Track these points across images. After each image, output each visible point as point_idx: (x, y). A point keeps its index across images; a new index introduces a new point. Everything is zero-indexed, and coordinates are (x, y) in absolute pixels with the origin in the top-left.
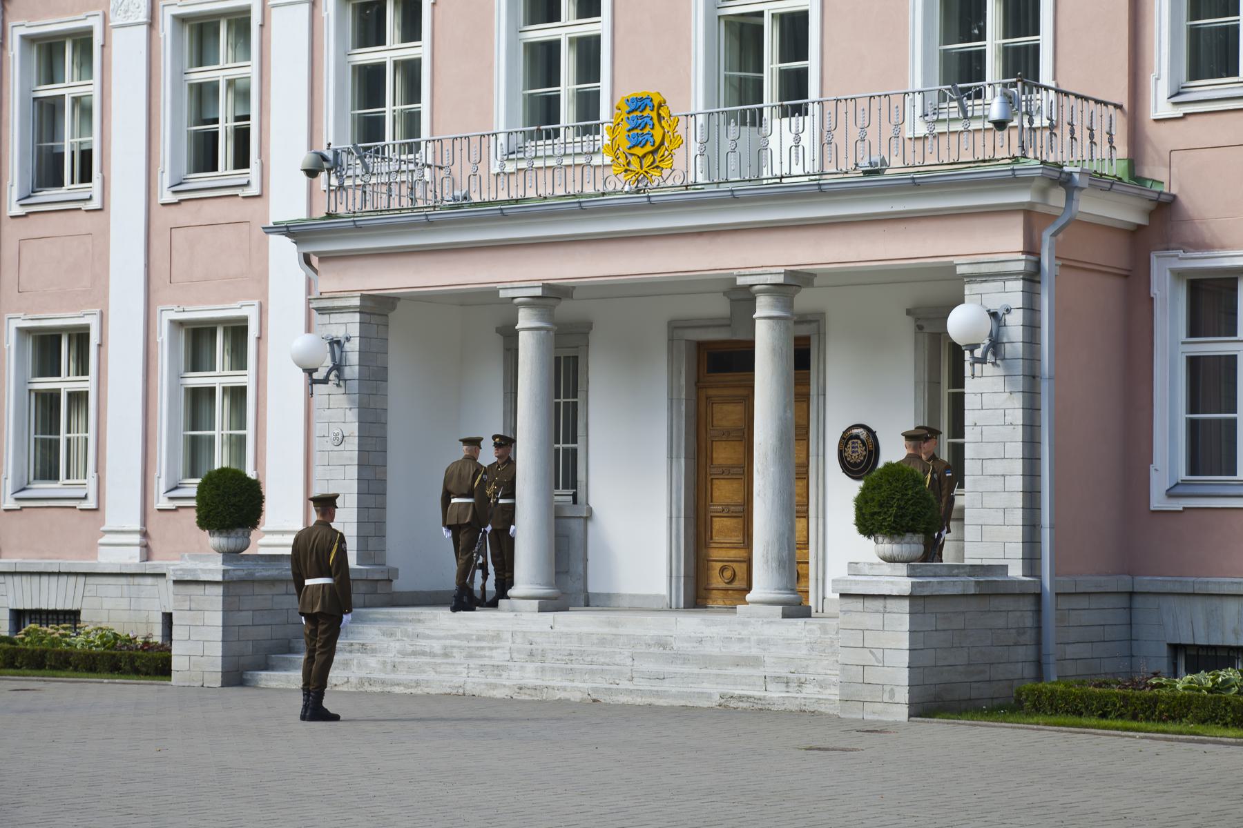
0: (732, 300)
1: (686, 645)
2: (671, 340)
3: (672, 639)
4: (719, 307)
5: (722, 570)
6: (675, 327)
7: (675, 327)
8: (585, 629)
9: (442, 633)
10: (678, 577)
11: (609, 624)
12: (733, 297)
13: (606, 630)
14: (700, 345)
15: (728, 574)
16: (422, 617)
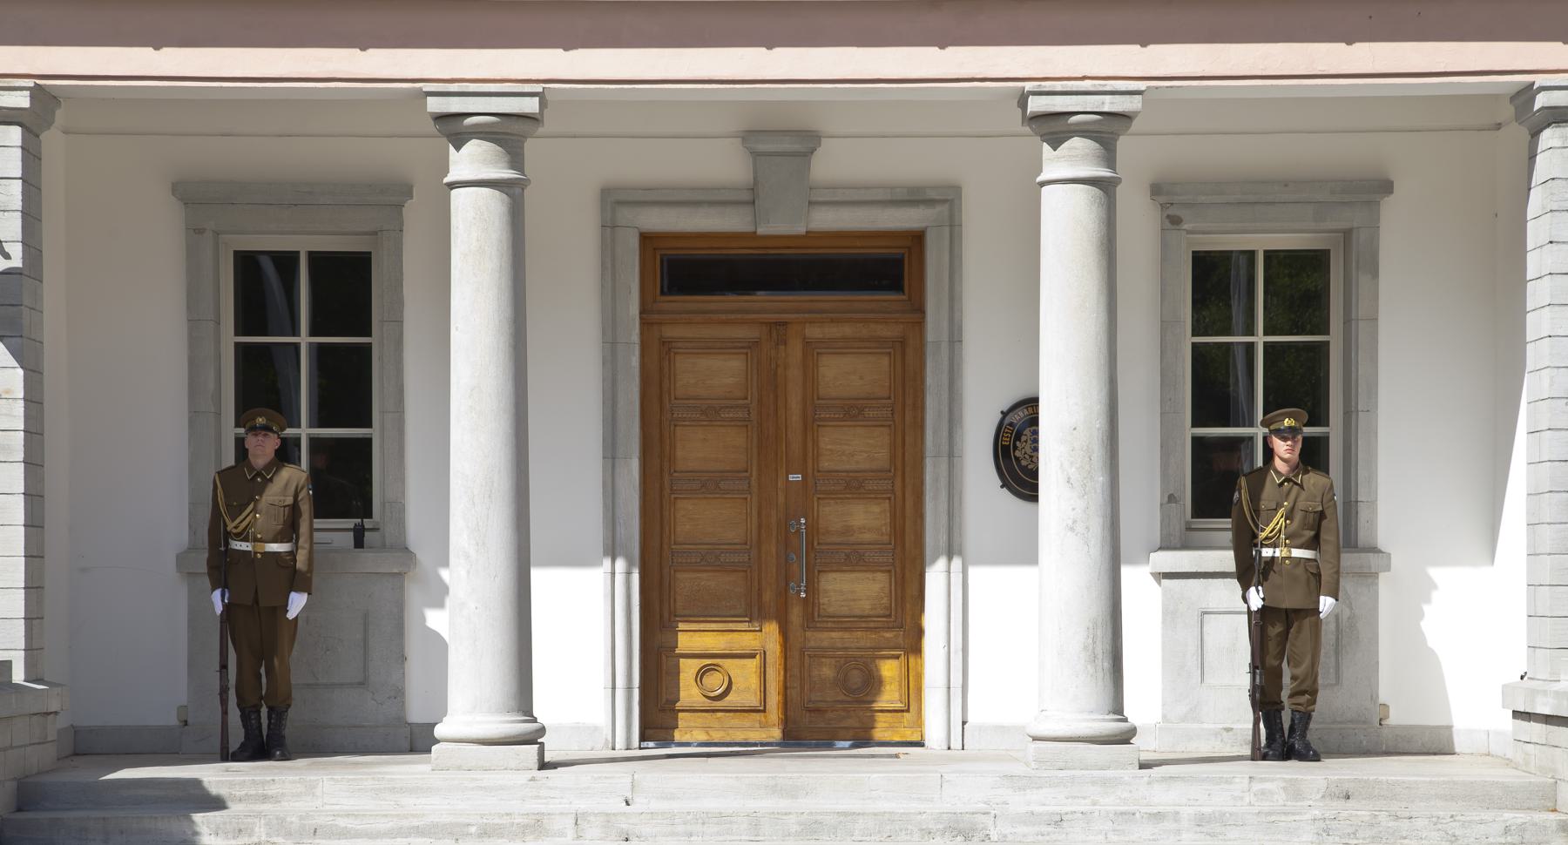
0: (756, 155)
1: (1022, 829)
2: (609, 227)
3: (989, 821)
4: (724, 165)
5: (701, 674)
6: (614, 200)
7: (614, 200)
8: (711, 804)
9: (383, 825)
10: (629, 688)
11: (775, 790)
12: (762, 147)
13: (766, 804)
14: (648, 240)
15: (715, 682)
16: (272, 790)
